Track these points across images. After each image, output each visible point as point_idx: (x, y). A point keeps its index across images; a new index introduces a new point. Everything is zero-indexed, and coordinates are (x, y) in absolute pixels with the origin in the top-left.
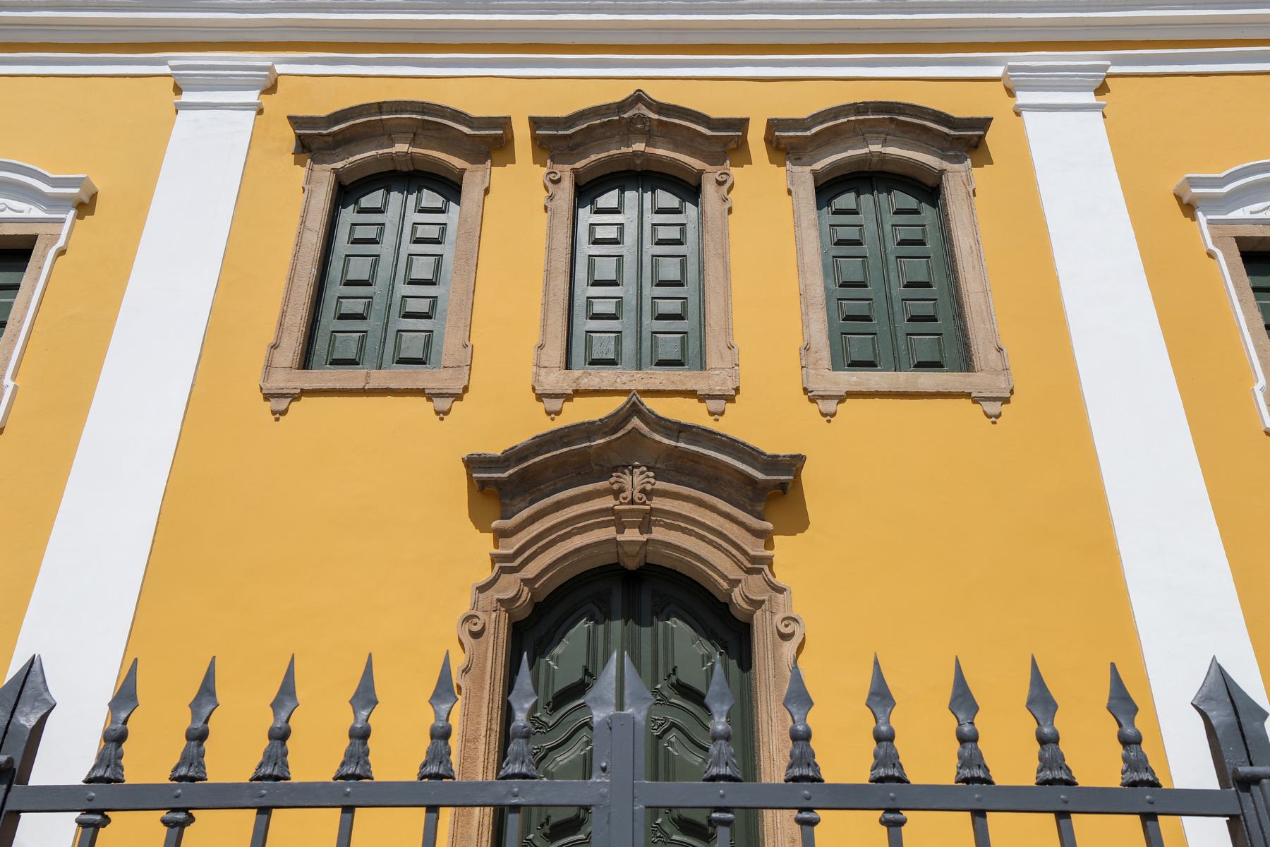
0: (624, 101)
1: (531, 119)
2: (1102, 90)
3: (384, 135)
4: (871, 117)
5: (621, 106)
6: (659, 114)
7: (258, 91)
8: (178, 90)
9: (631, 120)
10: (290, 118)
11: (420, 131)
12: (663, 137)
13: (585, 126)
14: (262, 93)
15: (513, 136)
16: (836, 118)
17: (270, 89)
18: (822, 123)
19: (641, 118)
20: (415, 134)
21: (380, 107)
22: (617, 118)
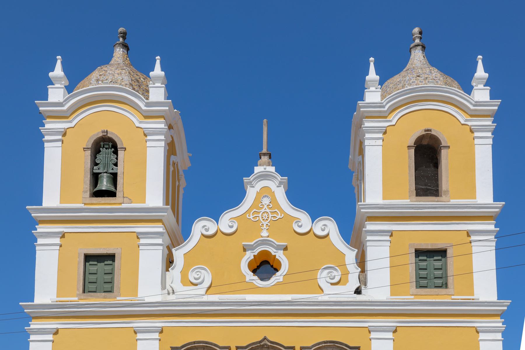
0: (261, 340)
1: (236, 347)
2: (395, 331)
3: (195, 348)
4: (328, 344)
5: (260, 342)
6: (271, 343)
7: (158, 333)
8: (136, 333)
9: (263, 345)
10: (171, 347)
11: (205, 347)
12: (272, 348)
13: (251, 347)
14: (159, 333)
15: (231, 348)
16: (319, 345)
17: (161, 332)
18: (315, 346)
19: (266, 344)
20: (204, 348)
21: (194, 343)
22: (259, 345)
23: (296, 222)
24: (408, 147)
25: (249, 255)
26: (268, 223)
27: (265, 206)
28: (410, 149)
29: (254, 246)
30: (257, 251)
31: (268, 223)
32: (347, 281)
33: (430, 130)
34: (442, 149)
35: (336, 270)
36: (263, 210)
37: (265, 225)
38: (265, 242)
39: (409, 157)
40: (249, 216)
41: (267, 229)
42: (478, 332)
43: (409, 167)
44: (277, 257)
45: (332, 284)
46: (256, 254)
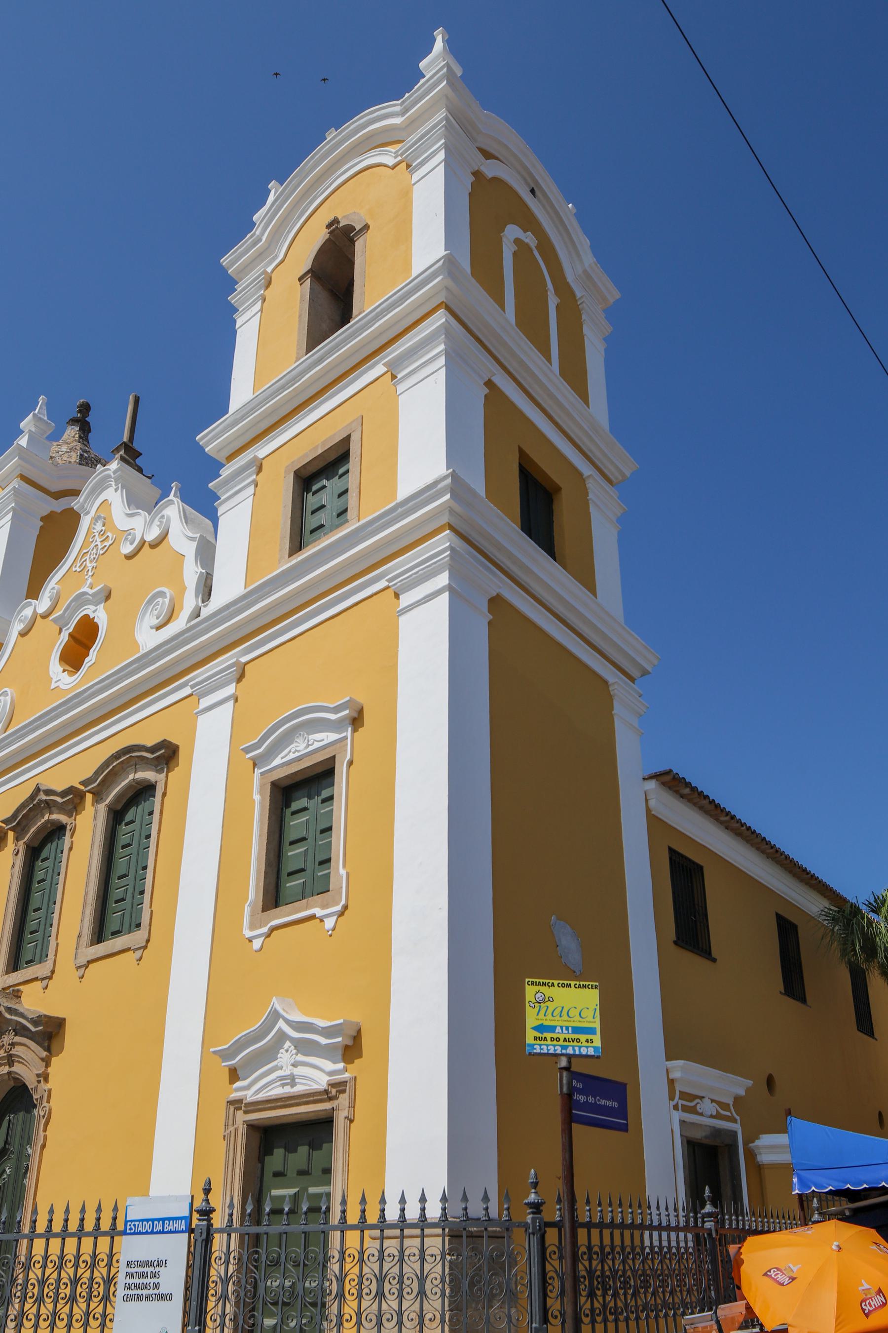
23: (126, 539)
24: (300, 279)
25: (65, 636)
26: (96, 562)
27: (97, 534)
28: (304, 282)
29: (66, 615)
30: (71, 627)
31: (96, 562)
32: (182, 608)
33: (336, 221)
34: (356, 241)
35: (162, 594)
36: (93, 545)
37: (90, 568)
38: (81, 600)
39: (302, 296)
40: (76, 567)
41: (92, 576)
42: (397, 596)
43: (300, 316)
44: (95, 620)
45: (158, 628)
46: (71, 630)
